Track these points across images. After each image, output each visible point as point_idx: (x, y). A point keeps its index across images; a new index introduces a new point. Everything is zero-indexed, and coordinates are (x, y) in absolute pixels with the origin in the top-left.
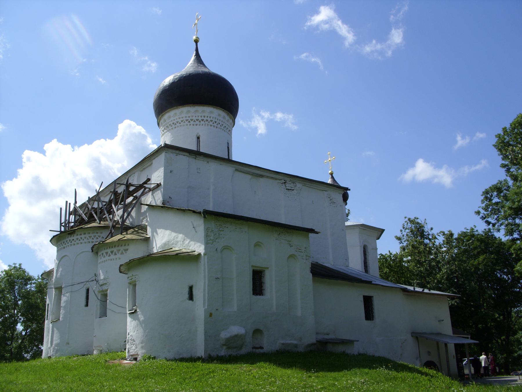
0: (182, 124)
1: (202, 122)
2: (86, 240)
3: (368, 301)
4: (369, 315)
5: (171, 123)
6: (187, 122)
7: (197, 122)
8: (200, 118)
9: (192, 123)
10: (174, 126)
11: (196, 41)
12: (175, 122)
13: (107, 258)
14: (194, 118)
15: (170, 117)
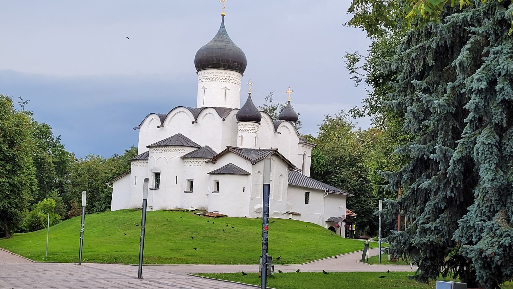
0: (217, 80)
1: (228, 81)
2: (175, 151)
3: (307, 194)
4: (307, 202)
5: (210, 77)
6: (220, 79)
7: (226, 80)
8: (227, 78)
9: (223, 80)
10: (211, 80)
11: (223, 16)
12: (212, 77)
13: (193, 164)
14: (224, 78)
15: (209, 73)
